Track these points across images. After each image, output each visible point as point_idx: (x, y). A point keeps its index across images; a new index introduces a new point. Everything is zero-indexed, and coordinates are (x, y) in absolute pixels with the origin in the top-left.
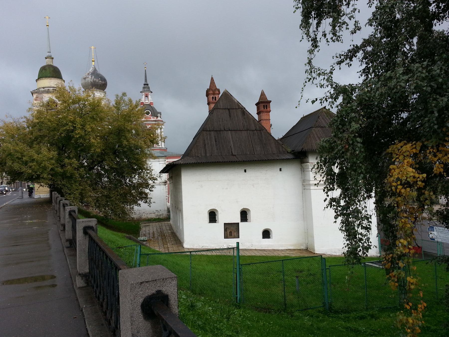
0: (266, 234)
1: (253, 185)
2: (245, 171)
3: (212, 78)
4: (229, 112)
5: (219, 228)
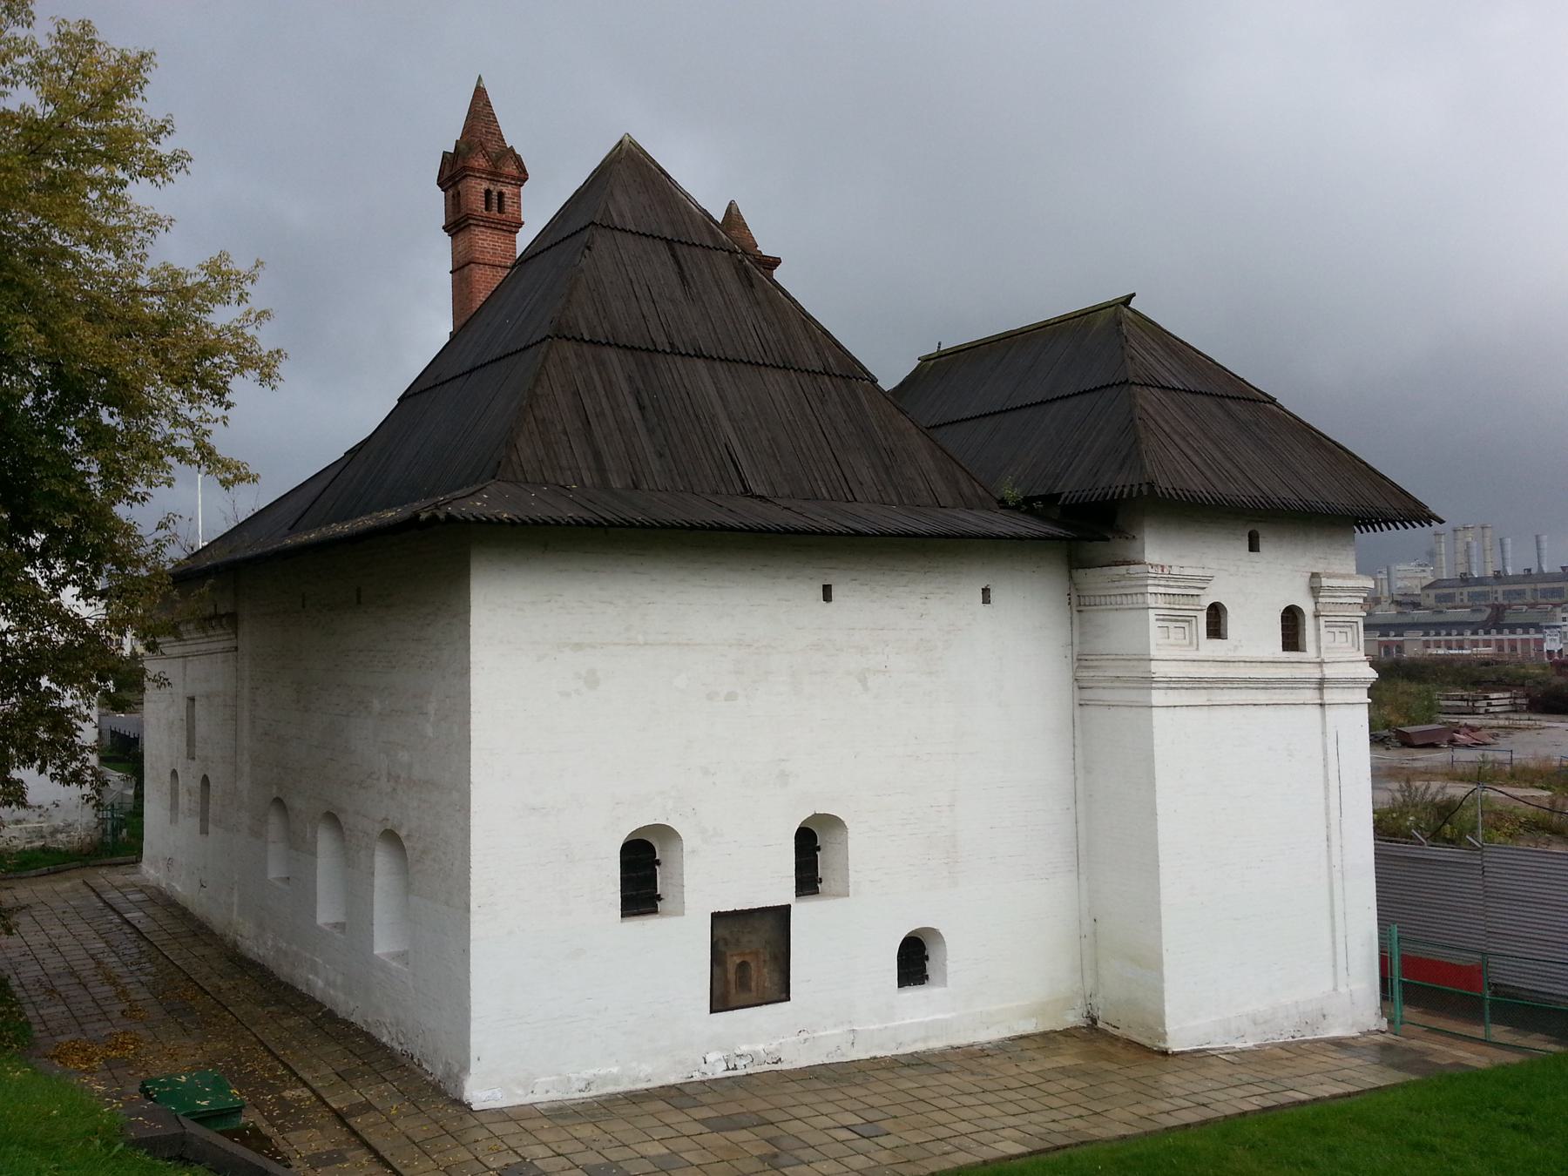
0: (914, 960)
1: (863, 681)
2: (827, 594)
3: (480, 94)
4: (674, 256)
5: (680, 943)
